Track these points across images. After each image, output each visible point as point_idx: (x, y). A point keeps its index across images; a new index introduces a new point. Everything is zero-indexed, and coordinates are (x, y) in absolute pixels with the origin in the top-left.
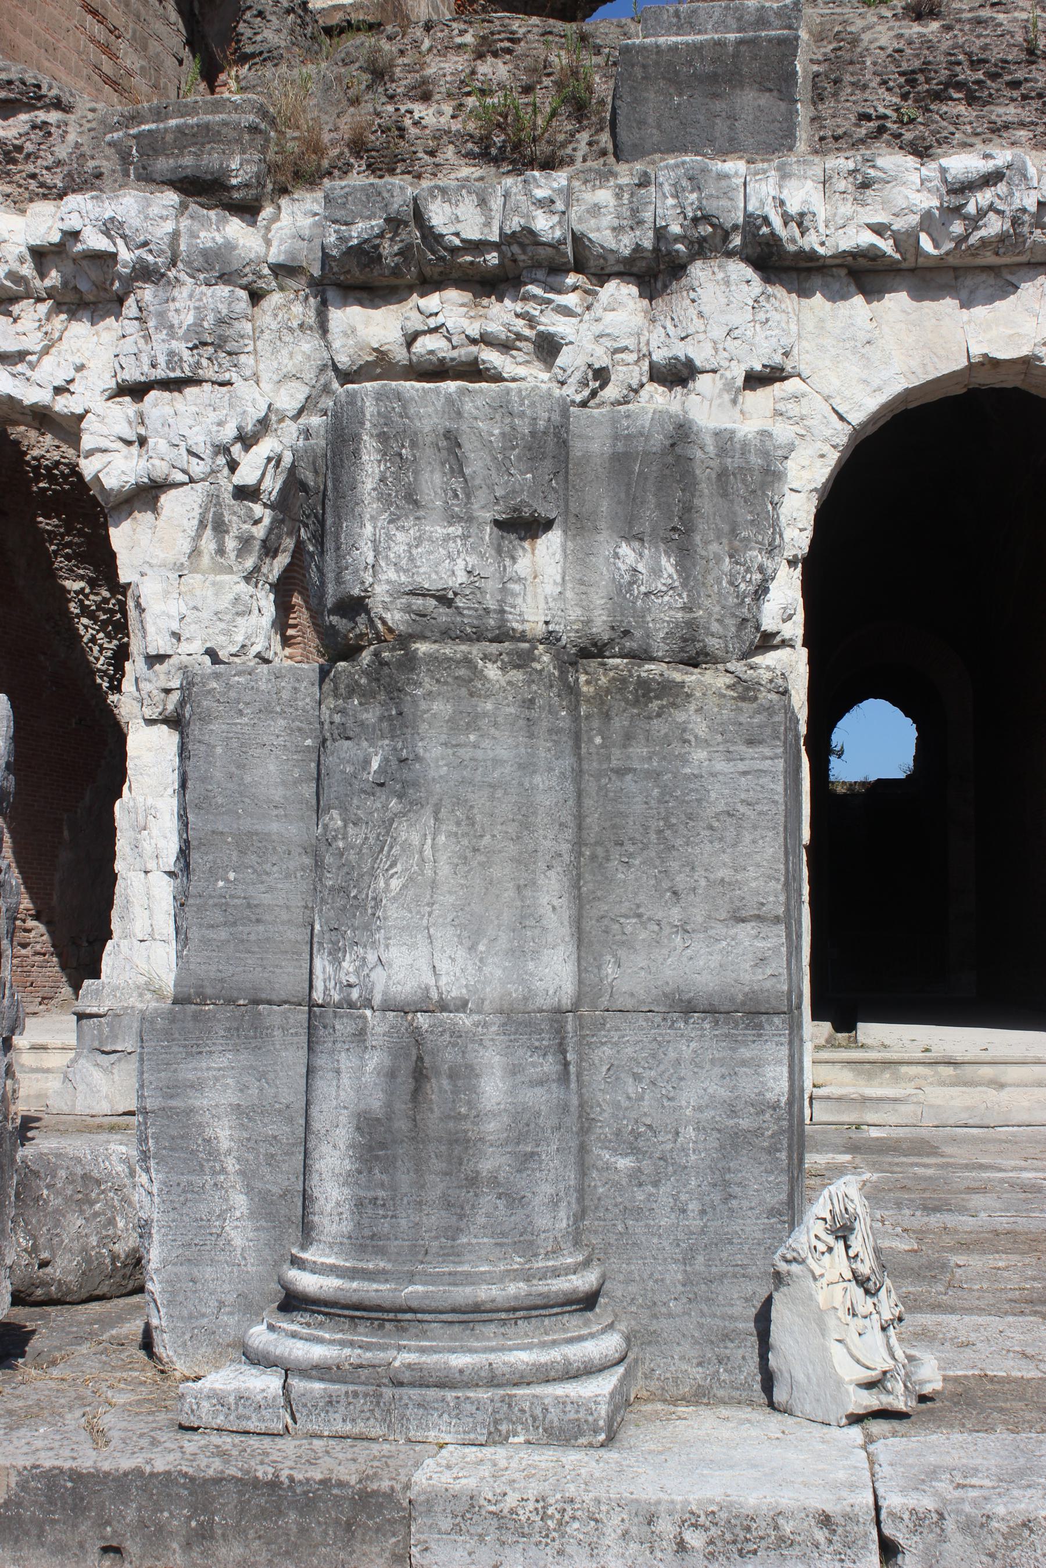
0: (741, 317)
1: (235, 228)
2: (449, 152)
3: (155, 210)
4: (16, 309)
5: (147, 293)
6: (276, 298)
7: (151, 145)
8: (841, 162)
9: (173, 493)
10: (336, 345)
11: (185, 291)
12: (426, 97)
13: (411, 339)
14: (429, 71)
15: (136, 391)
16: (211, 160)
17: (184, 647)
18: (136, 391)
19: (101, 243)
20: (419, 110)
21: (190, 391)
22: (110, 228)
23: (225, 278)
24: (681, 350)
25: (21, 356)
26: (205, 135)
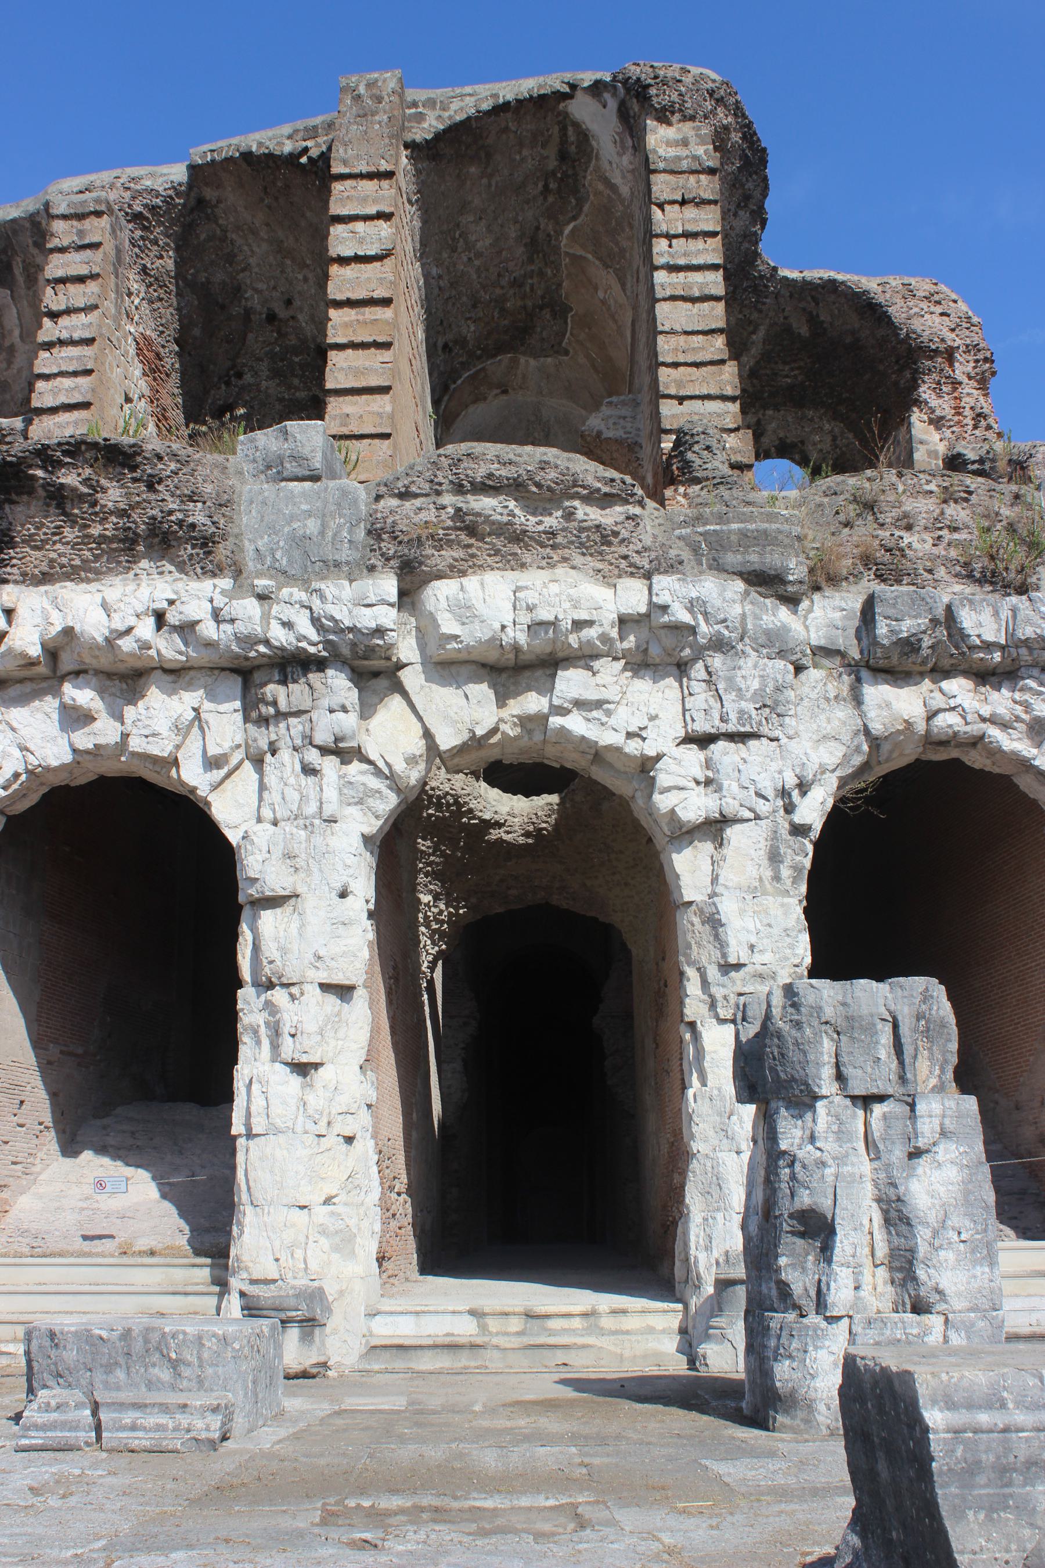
1: (784, 613)
2: (941, 572)
3: (729, 595)
4: (596, 664)
5: (717, 661)
6: (814, 674)
7: (718, 543)
9: (738, 827)
10: (872, 714)
11: (750, 662)
12: (909, 528)
13: (931, 716)
14: (907, 508)
15: (704, 741)
16: (772, 560)
17: (758, 958)
18: (704, 741)
19: (684, 616)
20: (908, 538)
21: (753, 743)
23: (781, 654)
25: (599, 704)
26: (764, 539)
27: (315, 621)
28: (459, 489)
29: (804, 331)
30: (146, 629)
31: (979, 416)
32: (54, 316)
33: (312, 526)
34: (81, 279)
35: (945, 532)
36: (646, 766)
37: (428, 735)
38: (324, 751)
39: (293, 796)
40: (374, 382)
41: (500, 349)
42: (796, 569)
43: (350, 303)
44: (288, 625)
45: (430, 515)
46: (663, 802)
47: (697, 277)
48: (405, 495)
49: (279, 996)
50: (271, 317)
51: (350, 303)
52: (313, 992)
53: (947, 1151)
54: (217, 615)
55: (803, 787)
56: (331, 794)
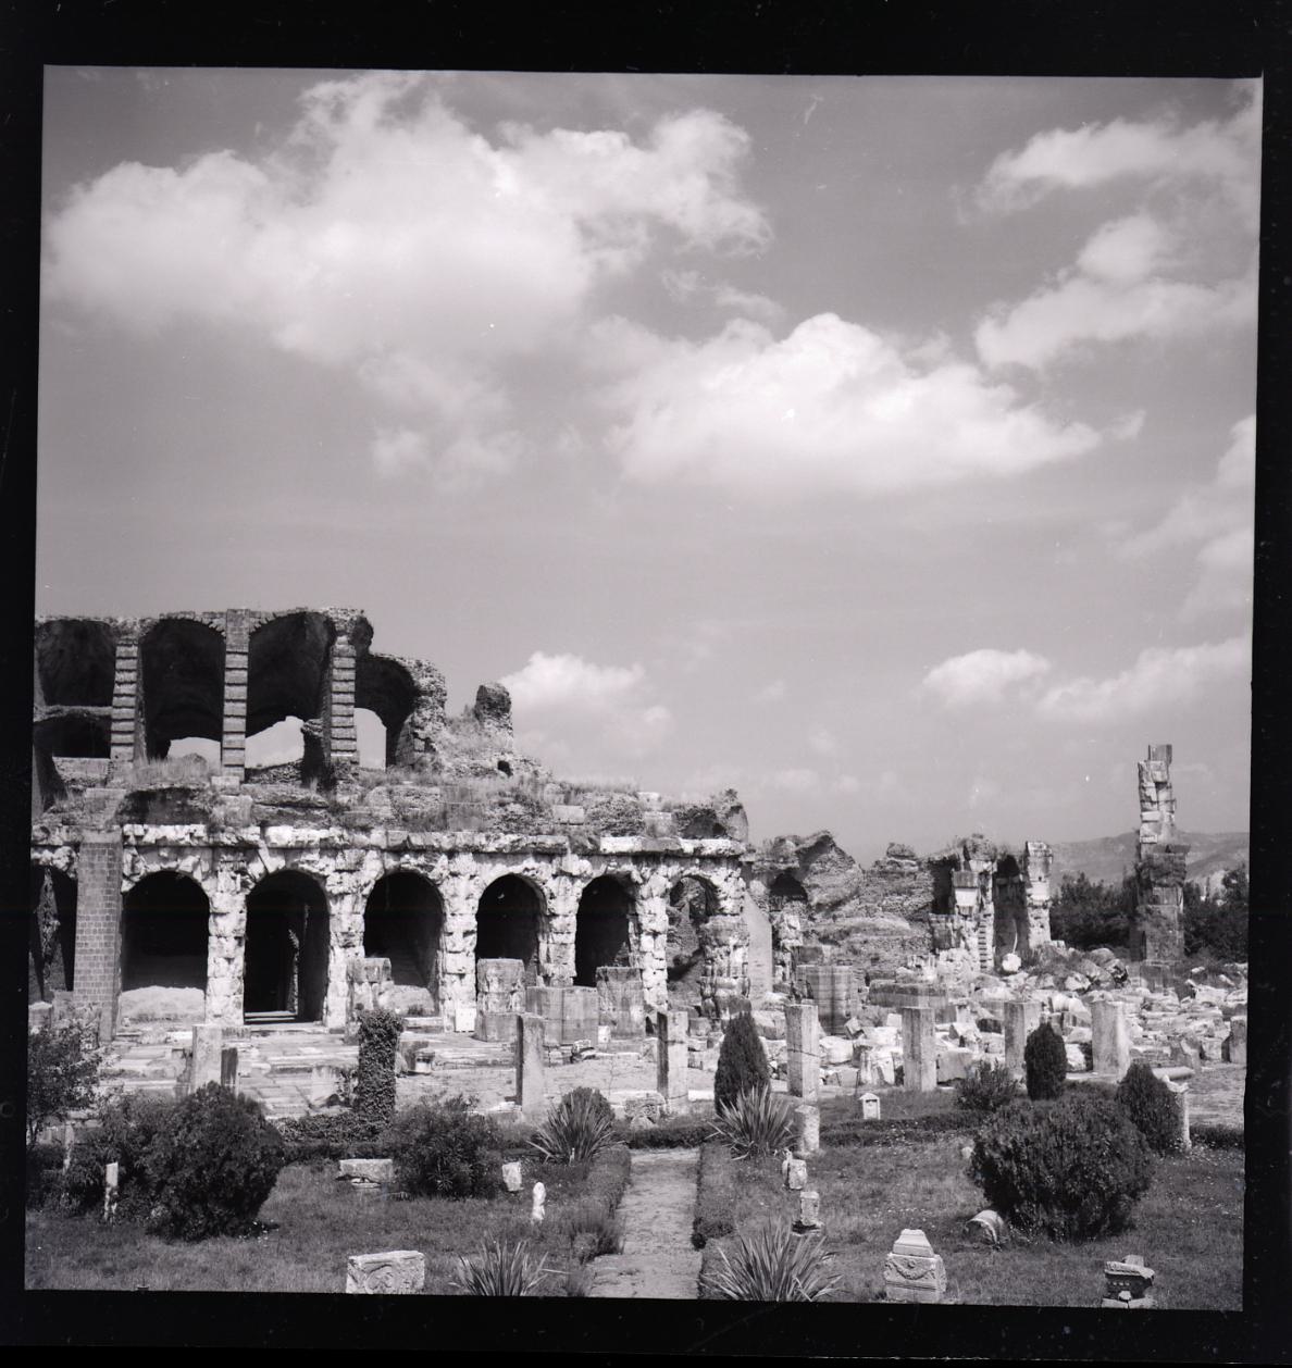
15: (340, 871)
18: (340, 871)
25: (313, 862)
30: (188, 839)
36: (325, 878)
37: (265, 867)
44: (229, 839)
46: (328, 889)
49: (222, 940)
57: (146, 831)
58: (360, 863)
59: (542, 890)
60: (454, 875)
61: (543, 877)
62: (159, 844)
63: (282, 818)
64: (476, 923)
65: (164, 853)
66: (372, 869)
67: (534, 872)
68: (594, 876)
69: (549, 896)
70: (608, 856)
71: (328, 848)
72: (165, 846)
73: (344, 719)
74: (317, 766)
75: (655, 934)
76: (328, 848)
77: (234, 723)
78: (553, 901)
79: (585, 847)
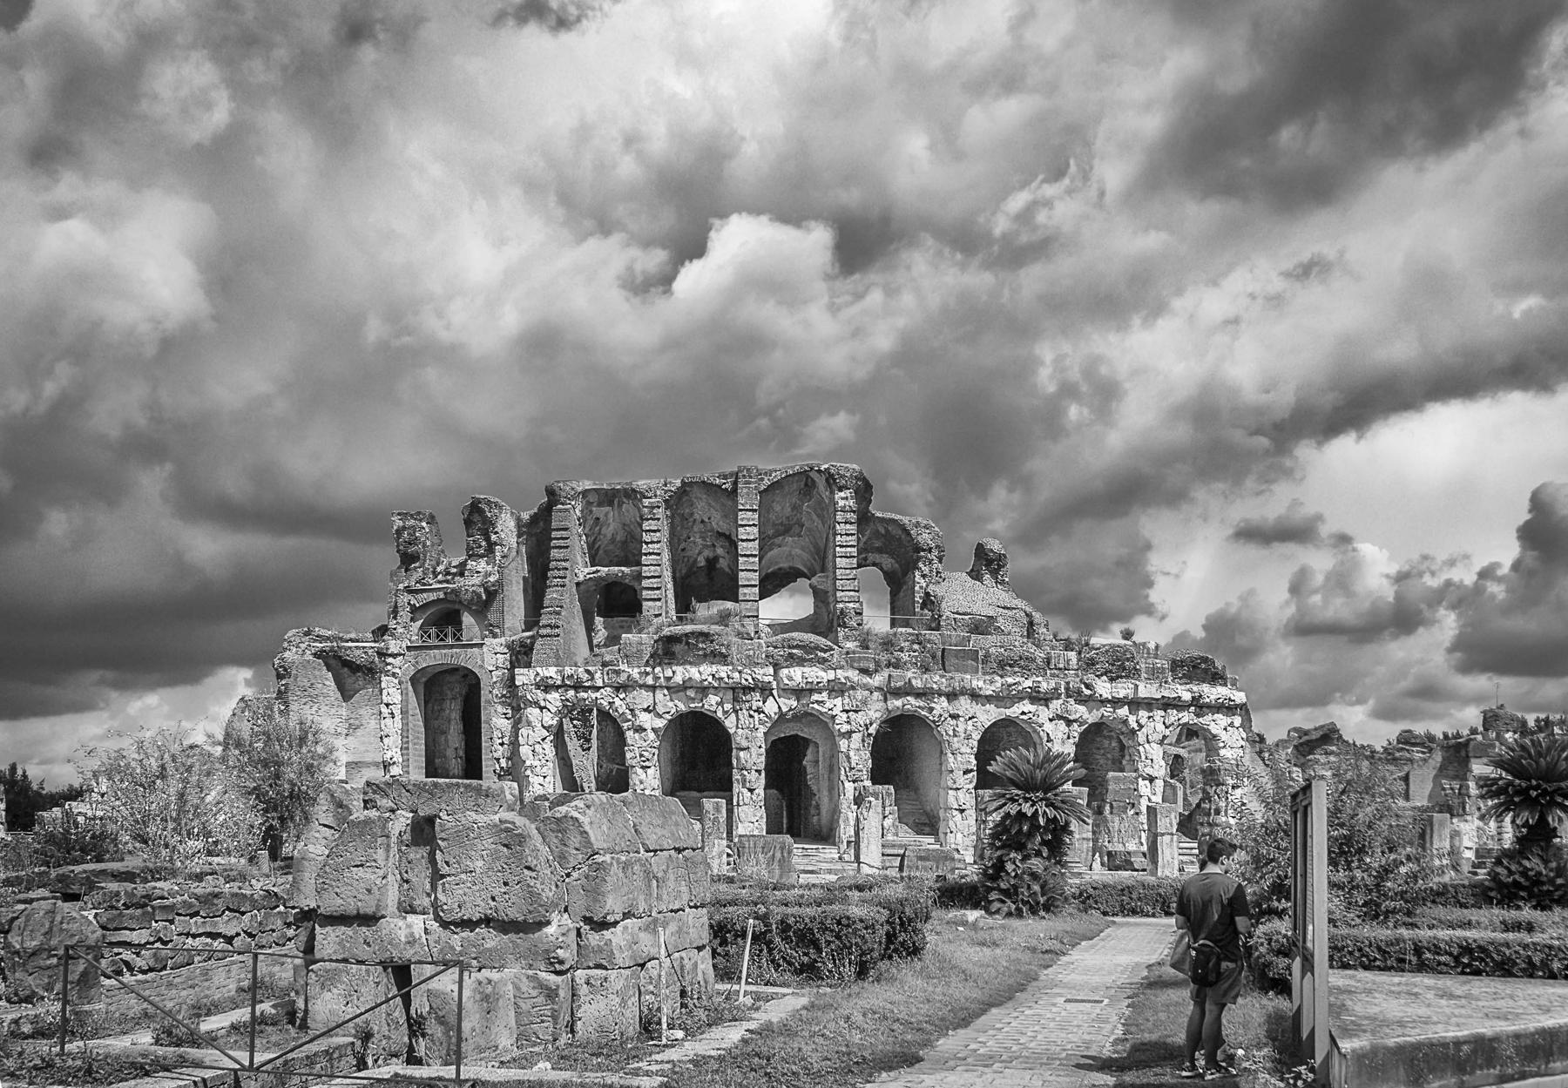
0: (968, 706)
7: (853, 660)
8: (987, 677)
15: (847, 711)
18: (847, 711)
20: (902, 655)
22: (846, 678)
24: (956, 712)
26: (867, 659)
27: (753, 679)
28: (789, 647)
29: (883, 532)
30: (710, 679)
31: (938, 572)
32: (647, 543)
33: (751, 653)
34: (654, 531)
35: (912, 653)
36: (833, 717)
37: (779, 707)
38: (755, 711)
39: (747, 722)
40: (753, 583)
41: (780, 535)
42: (872, 666)
43: (745, 555)
44: (746, 680)
45: (782, 653)
47: (849, 549)
48: (775, 647)
50: (703, 521)
51: (745, 555)
52: (753, 772)
53: (890, 816)
54: (728, 677)
55: (871, 724)
56: (757, 723)
57: (674, 672)
58: (865, 703)
59: (1039, 733)
60: (955, 717)
61: (1040, 721)
62: (685, 686)
63: (793, 660)
64: (975, 762)
65: (691, 693)
66: (875, 712)
67: (1031, 715)
68: (1090, 721)
69: (1046, 739)
70: (1104, 702)
71: (836, 689)
72: (691, 688)
73: (848, 571)
74: (826, 621)
75: (1152, 779)
76: (836, 689)
77: (749, 578)
78: (1049, 745)
79: (1079, 692)
